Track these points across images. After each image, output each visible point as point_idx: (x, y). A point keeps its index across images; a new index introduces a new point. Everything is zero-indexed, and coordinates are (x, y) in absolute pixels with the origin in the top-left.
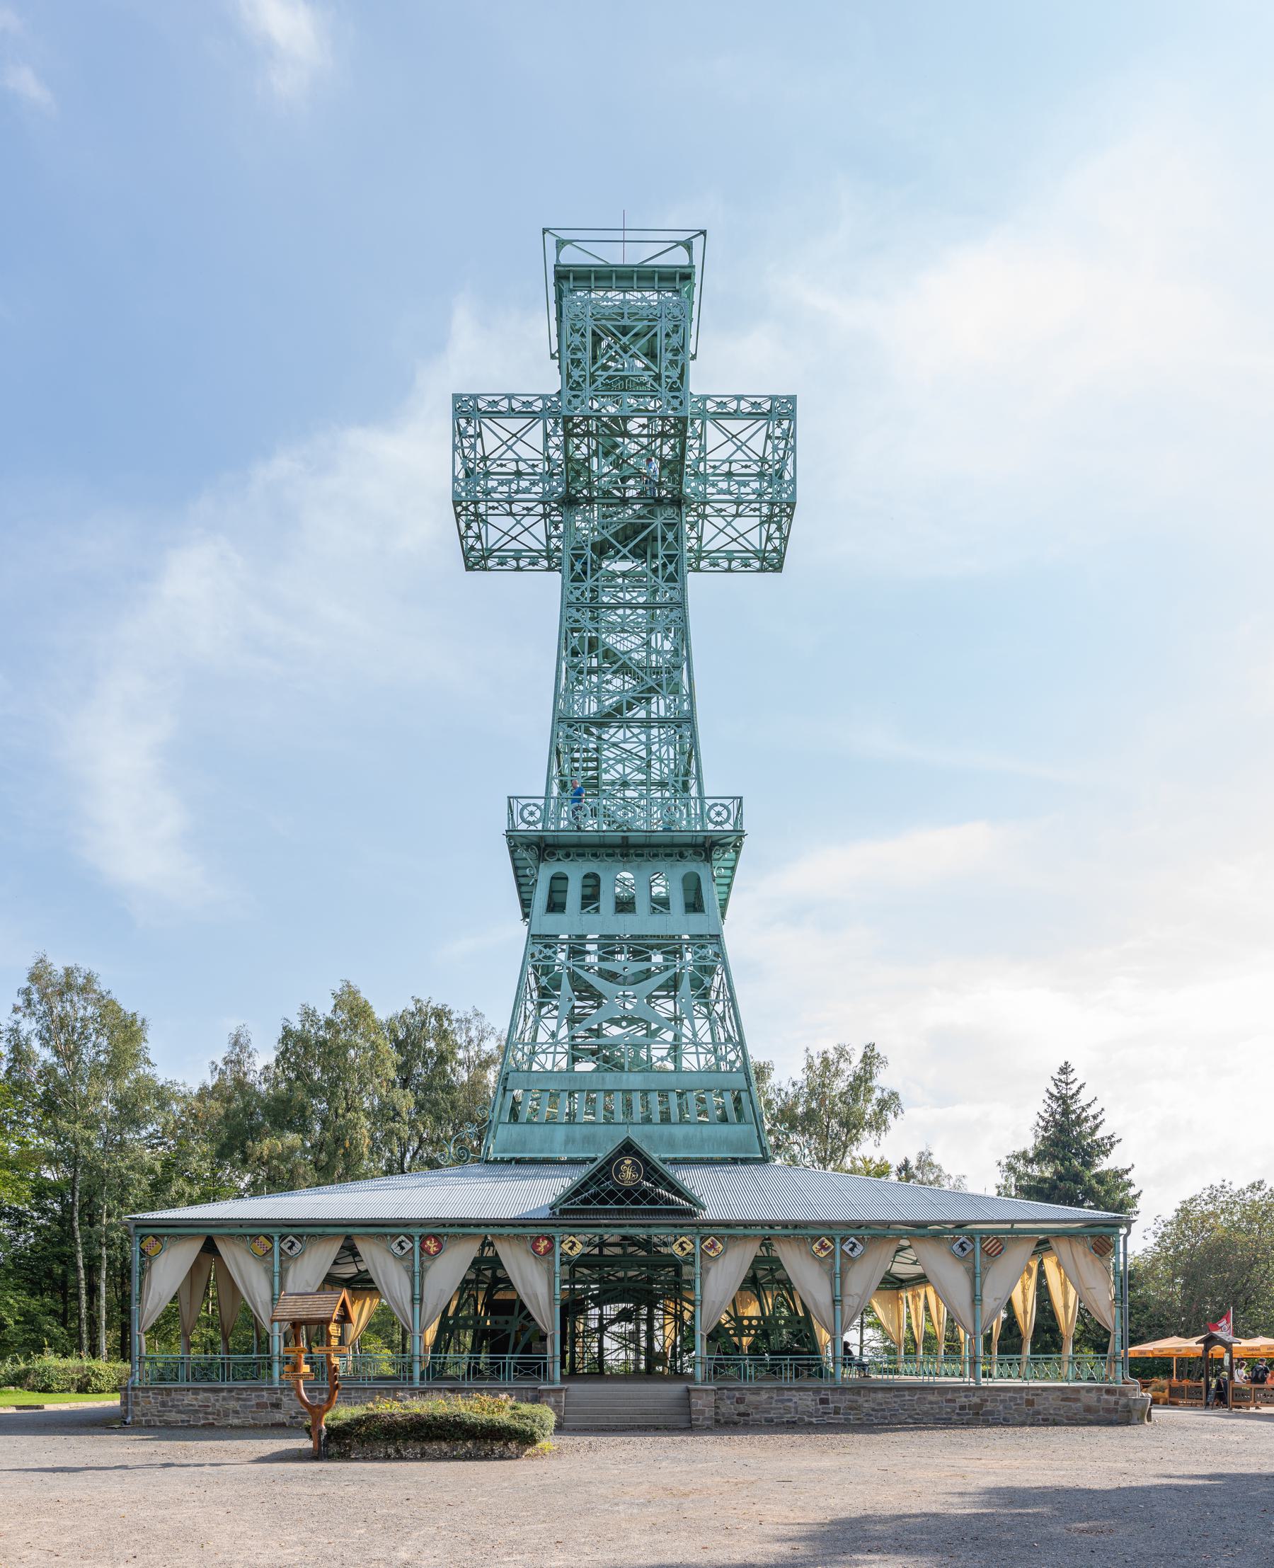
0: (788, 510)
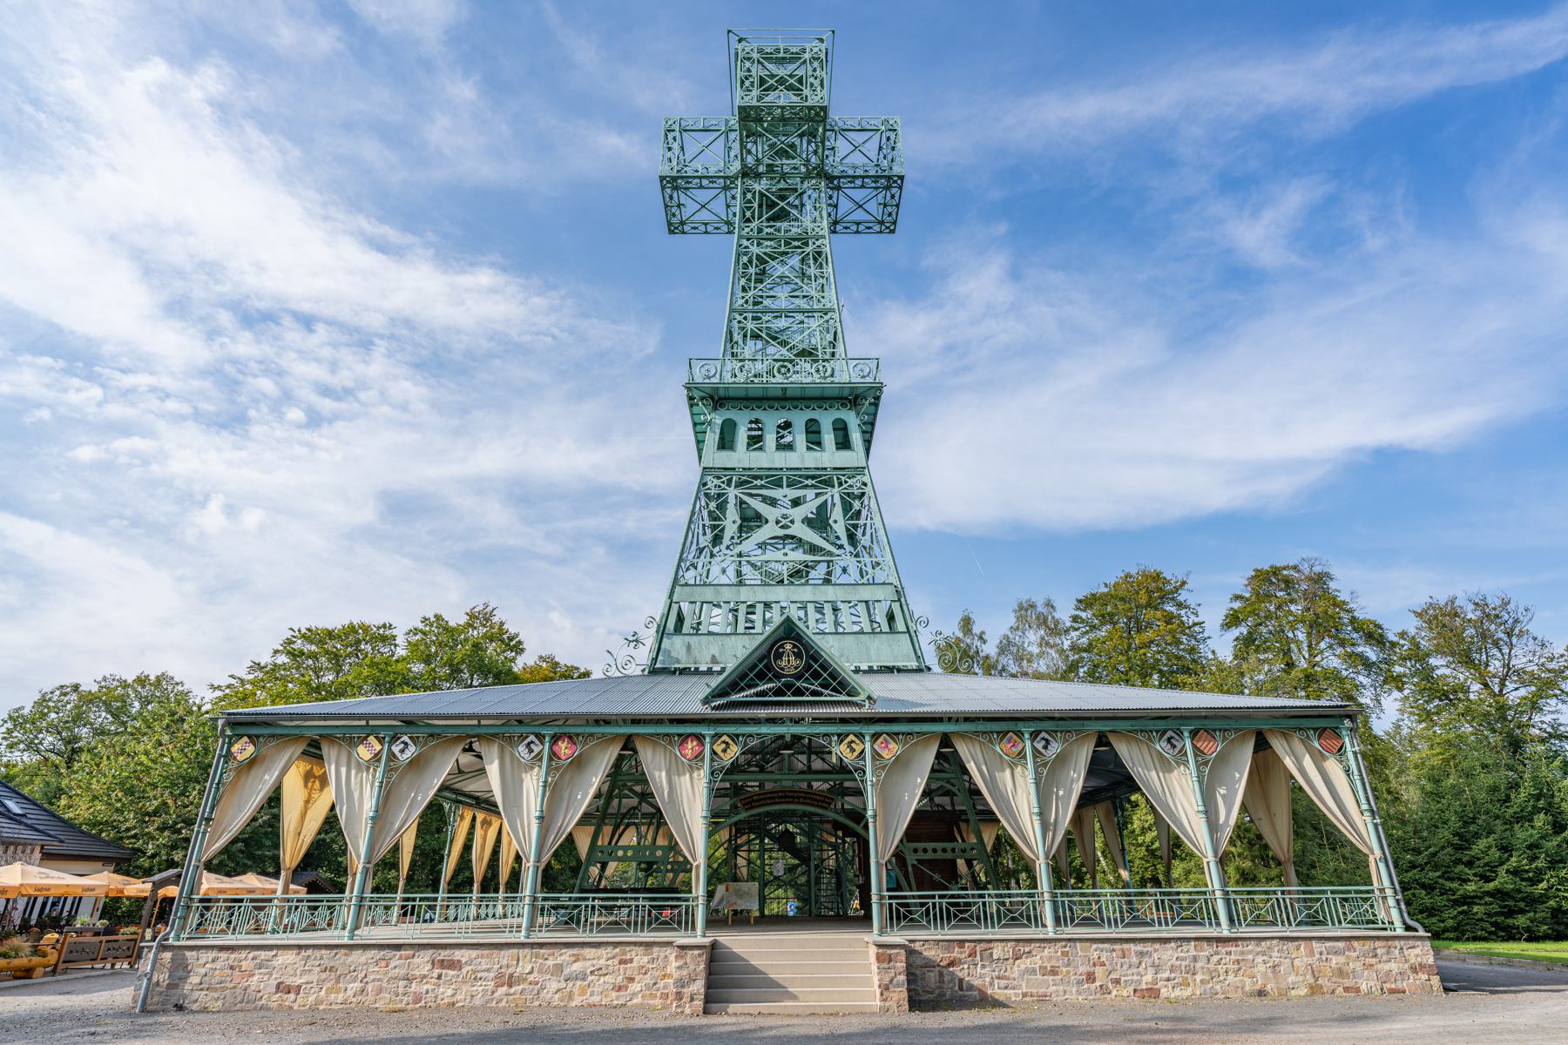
0: (899, 182)
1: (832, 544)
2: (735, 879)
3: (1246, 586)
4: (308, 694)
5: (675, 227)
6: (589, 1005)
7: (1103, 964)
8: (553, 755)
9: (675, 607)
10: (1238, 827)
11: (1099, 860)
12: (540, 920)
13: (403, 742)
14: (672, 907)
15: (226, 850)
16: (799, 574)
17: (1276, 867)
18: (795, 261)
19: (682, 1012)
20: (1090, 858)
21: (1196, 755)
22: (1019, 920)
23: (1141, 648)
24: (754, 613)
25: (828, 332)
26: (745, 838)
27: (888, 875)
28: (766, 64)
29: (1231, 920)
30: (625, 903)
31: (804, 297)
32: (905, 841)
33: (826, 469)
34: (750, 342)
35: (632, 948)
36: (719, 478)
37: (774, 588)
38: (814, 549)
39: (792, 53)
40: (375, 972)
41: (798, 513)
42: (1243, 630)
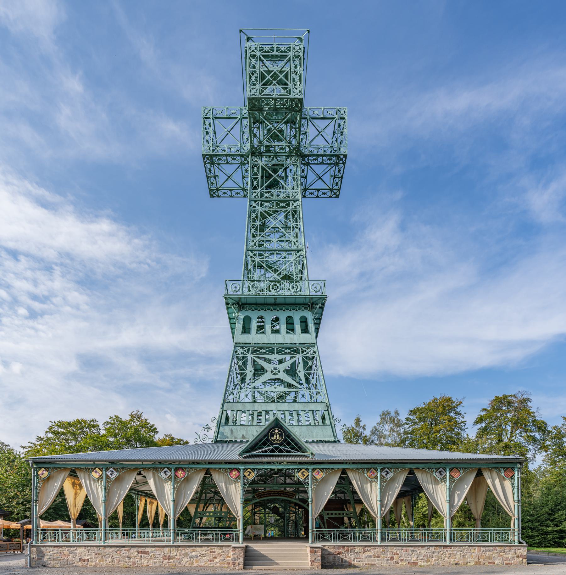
1: (298, 383)
2: (255, 524)
3: (490, 404)
4: (65, 450)
5: (214, 193)
6: (200, 566)
7: (398, 554)
8: (176, 477)
9: (225, 413)
10: (461, 506)
11: (402, 518)
12: (178, 538)
13: (111, 471)
14: (230, 534)
15: (46, 512)
16: (282, 397)
17: (473, 521)
18: (281, 217)
19: (235, 569)
20: (399, 517)
21: (450, 478)
22: (367, 539)
23: (435, 433)
24: (261, 416)
25: (299, 264)
26: (258, 509)
27: (316, 523)
28: (265, 61)
29: (451, 540)
30: (211, 532)
31: (287, 241)
32: (324, 510)
33: (296, 344)
34: (257, 270)
35: (215, 547)
36: (243, 348)
37: (270, 404)
38: (289, 385)
39: (282, 52)
40: (116, 555)
41: (282, 367)
42: (483, 425)
